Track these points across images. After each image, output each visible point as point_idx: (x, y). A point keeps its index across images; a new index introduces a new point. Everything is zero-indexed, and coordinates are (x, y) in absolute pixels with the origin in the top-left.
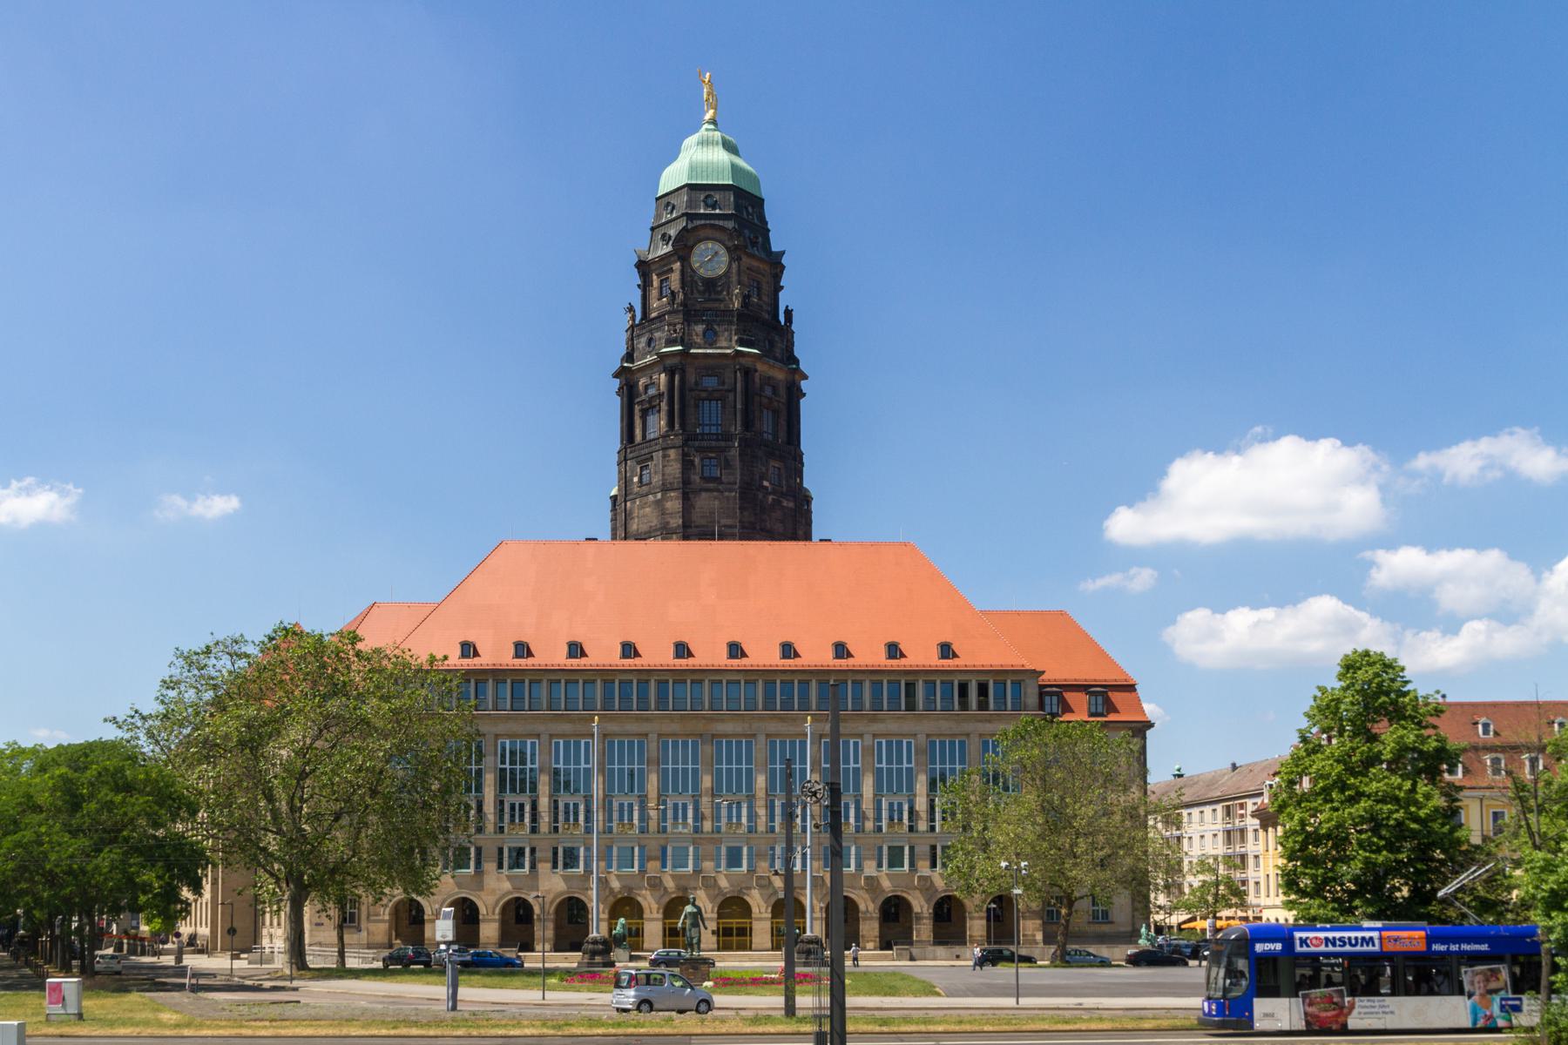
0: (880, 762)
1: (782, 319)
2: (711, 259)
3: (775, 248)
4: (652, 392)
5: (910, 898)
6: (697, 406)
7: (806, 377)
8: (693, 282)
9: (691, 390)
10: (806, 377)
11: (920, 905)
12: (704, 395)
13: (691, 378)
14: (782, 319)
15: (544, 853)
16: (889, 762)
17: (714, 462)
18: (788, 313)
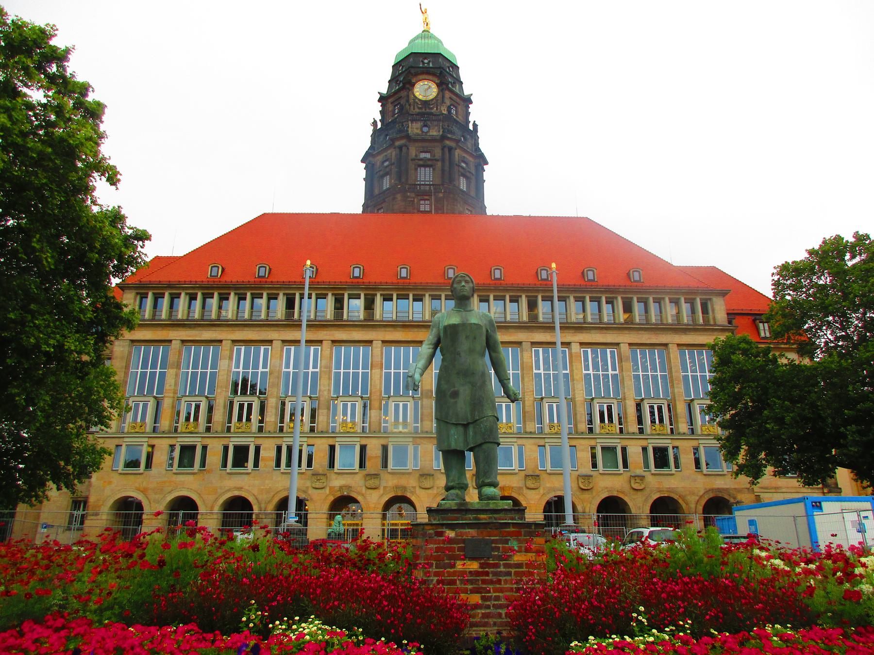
0: (587, 368)
1: (471, 127)
2: (425, 90)
3: (466, 92)
4: (386, 164)
5: (626, 499)
6: (416, 169)
7: (487, 163)
8: (415, 102)
9: (413, 160)
10: (487, 163)
11: (639, 506)
12: (421, 163)
13: (413, 152)
14: (471, 127)
15: (268, 453)
16: (596, 368)
17: (427, 202)
18: (475, 126)
